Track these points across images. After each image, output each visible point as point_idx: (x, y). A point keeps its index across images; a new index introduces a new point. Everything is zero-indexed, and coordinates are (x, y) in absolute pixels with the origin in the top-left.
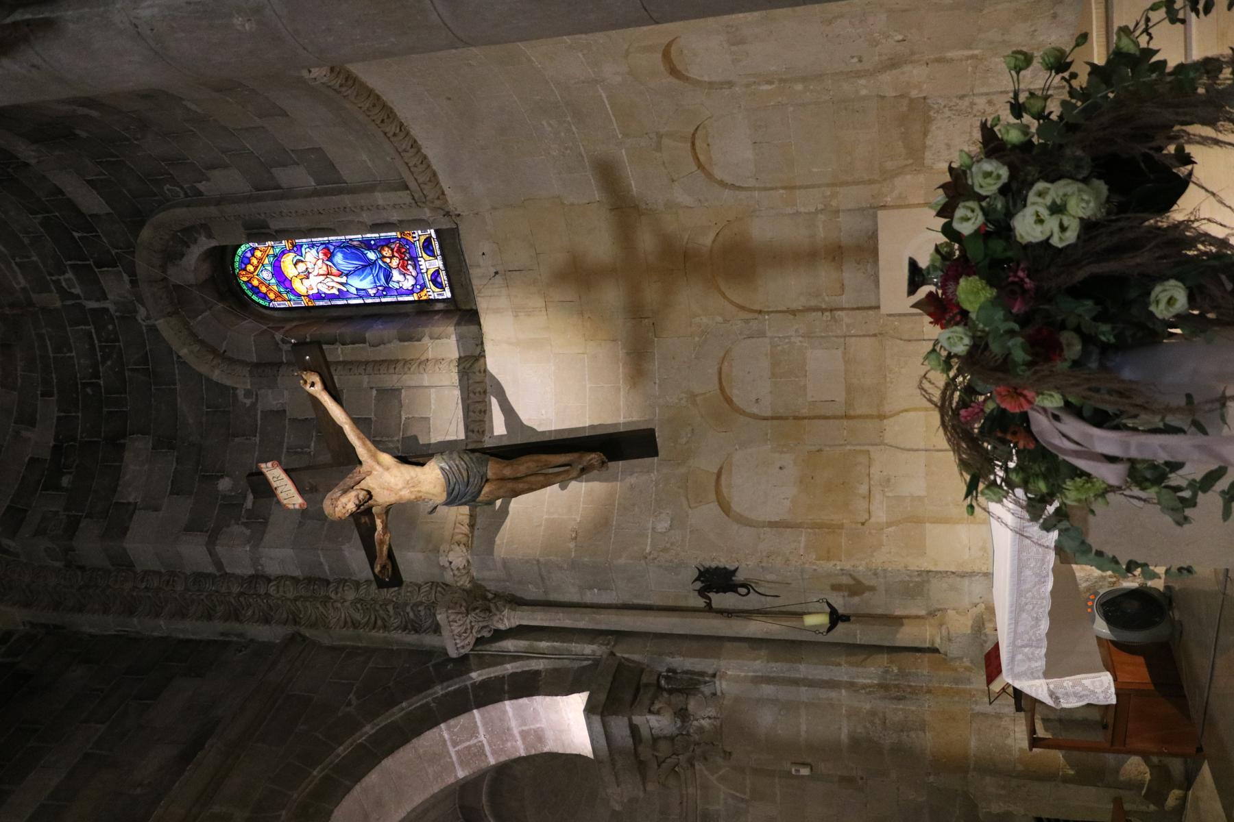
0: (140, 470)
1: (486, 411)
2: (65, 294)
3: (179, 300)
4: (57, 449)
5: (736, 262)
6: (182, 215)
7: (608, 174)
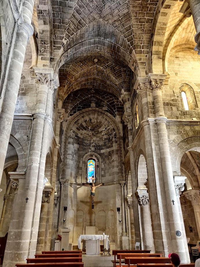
0: (76, 146)
1: (79, 185)
2: (93, 143)
3: (92, 155)
5: (90, 213)
6: (100, 160)
7: (100, 202)
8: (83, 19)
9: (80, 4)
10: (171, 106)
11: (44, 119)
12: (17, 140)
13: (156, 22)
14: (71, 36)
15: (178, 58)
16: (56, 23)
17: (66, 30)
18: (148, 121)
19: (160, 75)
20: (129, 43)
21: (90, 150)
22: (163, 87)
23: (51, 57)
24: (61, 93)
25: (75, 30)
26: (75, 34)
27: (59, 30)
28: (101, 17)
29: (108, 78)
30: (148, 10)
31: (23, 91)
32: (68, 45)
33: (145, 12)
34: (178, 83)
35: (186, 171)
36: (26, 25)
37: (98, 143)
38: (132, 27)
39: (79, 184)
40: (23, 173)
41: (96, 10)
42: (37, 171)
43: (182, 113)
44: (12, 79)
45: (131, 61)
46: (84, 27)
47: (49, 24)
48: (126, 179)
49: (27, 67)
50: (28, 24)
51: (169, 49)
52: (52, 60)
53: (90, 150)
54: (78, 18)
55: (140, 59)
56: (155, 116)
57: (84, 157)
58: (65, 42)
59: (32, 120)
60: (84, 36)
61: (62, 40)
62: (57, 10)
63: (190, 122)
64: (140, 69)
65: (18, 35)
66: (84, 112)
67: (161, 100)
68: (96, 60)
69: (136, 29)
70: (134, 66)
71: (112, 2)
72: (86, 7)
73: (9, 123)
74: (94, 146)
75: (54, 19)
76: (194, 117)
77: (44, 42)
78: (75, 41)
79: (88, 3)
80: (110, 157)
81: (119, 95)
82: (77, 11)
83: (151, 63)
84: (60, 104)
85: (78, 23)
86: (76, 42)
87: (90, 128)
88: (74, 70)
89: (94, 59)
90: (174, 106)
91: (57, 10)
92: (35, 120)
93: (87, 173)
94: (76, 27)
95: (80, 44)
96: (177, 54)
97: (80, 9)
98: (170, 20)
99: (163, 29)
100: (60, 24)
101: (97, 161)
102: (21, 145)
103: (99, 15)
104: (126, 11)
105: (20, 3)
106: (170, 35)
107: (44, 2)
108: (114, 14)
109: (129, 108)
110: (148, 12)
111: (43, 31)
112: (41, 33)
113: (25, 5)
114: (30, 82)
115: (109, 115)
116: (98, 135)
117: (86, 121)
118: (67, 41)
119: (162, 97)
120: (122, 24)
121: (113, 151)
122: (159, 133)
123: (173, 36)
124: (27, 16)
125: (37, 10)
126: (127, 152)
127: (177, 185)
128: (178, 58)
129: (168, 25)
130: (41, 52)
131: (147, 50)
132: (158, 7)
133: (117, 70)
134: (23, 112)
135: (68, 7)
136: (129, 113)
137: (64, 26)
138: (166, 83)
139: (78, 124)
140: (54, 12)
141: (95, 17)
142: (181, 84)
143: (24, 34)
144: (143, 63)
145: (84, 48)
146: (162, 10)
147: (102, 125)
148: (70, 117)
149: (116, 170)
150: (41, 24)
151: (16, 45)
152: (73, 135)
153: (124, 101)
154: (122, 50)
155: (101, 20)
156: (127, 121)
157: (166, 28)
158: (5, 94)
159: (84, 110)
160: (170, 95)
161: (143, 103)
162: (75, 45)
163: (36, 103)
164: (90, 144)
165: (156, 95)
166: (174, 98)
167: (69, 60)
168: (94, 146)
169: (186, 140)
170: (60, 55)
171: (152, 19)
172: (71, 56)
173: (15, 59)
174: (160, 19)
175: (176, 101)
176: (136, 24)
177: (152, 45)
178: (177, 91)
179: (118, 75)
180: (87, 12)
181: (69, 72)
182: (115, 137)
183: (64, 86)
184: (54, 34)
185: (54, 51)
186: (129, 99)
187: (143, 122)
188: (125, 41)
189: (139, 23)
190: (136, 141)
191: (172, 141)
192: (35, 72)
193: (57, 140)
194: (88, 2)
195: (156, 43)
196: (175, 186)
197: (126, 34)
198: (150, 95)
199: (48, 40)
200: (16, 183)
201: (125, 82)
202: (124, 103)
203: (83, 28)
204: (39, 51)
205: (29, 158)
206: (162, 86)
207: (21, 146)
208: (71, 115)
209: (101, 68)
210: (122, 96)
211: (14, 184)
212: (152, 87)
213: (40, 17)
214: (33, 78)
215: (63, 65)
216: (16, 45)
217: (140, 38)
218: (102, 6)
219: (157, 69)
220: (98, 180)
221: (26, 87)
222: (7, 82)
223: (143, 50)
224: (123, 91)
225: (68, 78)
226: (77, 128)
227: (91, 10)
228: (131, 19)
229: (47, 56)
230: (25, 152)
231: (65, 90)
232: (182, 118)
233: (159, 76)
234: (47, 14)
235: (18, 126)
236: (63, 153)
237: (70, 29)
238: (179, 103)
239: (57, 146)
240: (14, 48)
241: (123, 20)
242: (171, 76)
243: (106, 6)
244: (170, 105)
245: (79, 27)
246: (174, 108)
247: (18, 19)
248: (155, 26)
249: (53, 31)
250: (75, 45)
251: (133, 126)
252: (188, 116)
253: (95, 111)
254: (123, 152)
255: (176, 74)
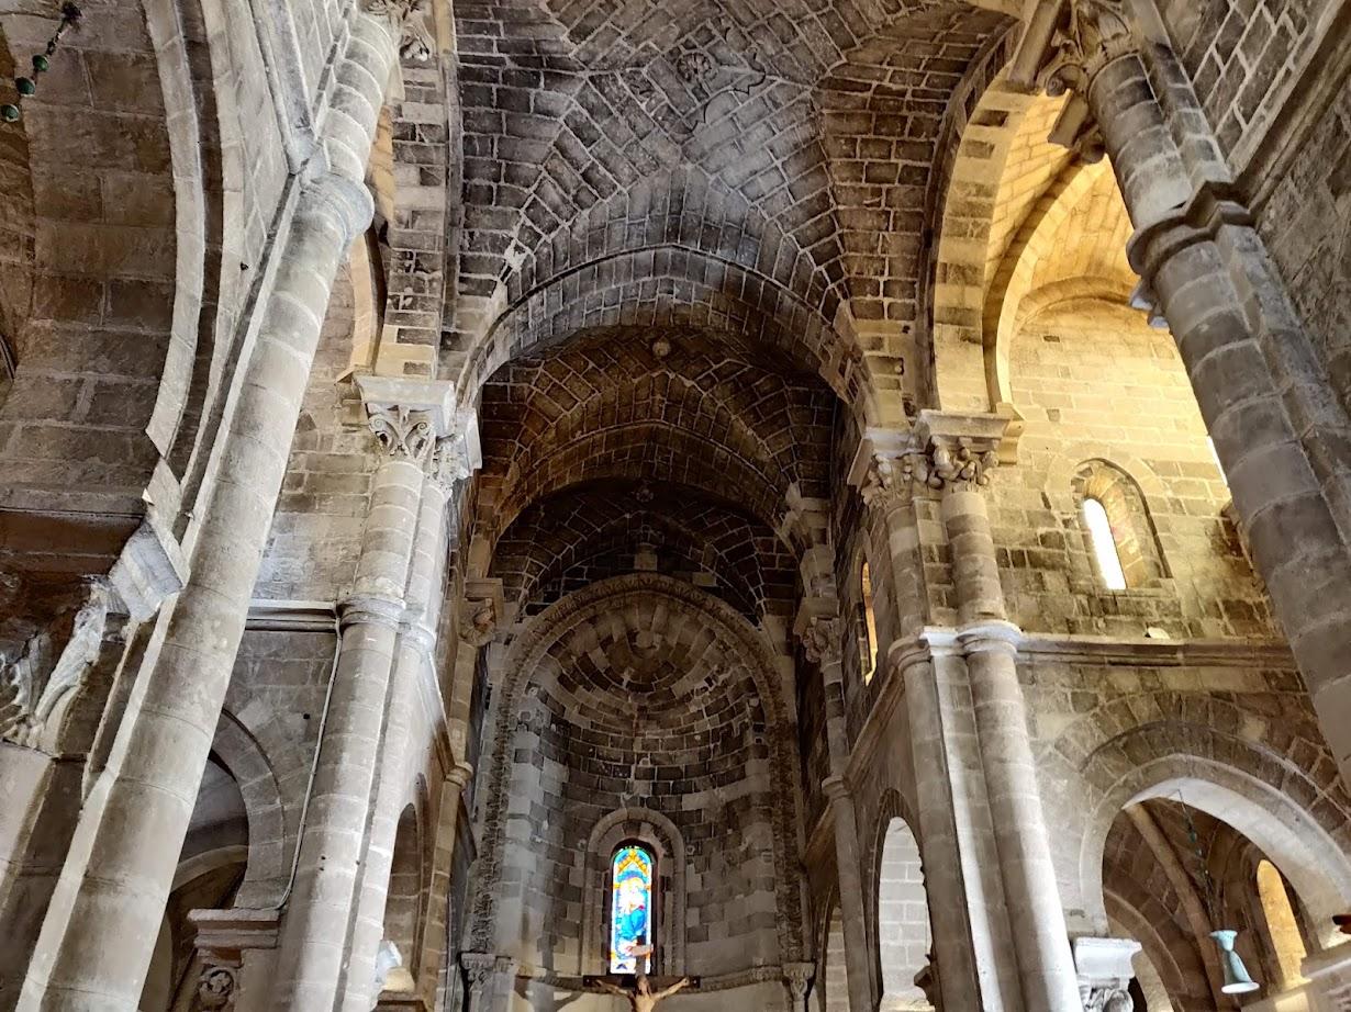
0: (554, 771)
1: (566, 988)
2: (640, 756)
3: (633, 824)
4: (566, 724)
6: (681, 850)
8: (605, 163)
9: (592, 99)
10: (1038, 570)
11: (397, 626)
12: (251, 736)
13: (946, 180)
14: (544, 237)
15: (1057, 339)
16: (476, 181)
17: (522, 211)
18: (923, 644)
19: (973, 419)
20: (822, 268)
21: (628, 797)
22: (993, 476)
23: (446, 329)
24: (486, 503)
25: (565, 210)
26: (566, 225)
27: (492, 207)
28: (686, 155)
29: (721, 429)
30: (907, 131)
31: (300, 491)
32: (528, 274)
33: (893, 139)
34: (1064, 457)
35: (1136, 913)
36: (341, 188)
37: (670, 758)
38: (831, 201)
39: (564, 984)
40: (269, 915)
41: (667, 125)
42: (345, 906)
43: (1093, 604)
44: (255, 427)
45: (830, 350)
46: (610, 199)
47: (444, 184)
48: (814, 950)
49: (326, 374)
50: (351, 183)
51: (1011, 299)
52: (449, 341)
53: (628, 797)
54: (580, 157)
55: (877, 344)
56: (959, 621)
57: (595, 833)
58: (514, 260)
59: (334, 631)
60: (609, 237)
61: (502, 252)
62: (487, 123)
63: (1139, 649)
64: (879, 391)
65: (299, 227)
66: (598, 598)
67: (982, 539)
68: (662, 348)
69: (851, 211)
70: (846, 374)
71: (740, 94)
72: (622, 112)
73: (225, 642)
74: (646, 775)
75: (466, 163)
76: (1155, 625)
77: (417, 263)
78: (566, 259)
79: (630, 98)
80: (730, 831)
81: (777, 515)
82: (578, 131)
83: (927, 361)
84: (481, 554)
85: (580, 178)
86: (568, 263)
87: (626, 678)
88: (556, 392)
89: (653, 341)
90: (1053, 567)
91: (487, 123)
92: (349, 632)
93: (606, 919)
94: (570, 198)
95: (587, 269)
96: (1050, 322)
97: (593, 123)
98: (1006, 175)
99: (978, 211)
100: (497, 180)
101: (660, 856)
102: (268, 762)
103: (679, 147)
104: (803, 133)
105: (320, 96)
106: (1012, 236)
107: (428, 93)
108: (747, 145)
109: (827, 576)
110: (906, 137)
111: (415, 213)
112: (405, 220)
113: (342, 102)
114: (336, 444)
115: (726, 610)
116: (672, 715)
117: (605, 643)
118: (524, 256)
119: (991, 520)
120: (785, 185)
121: (746, 799)
122: (981, 704)
123: (1026, 242)
124: (349, 150)
125: (395, 123)
126: (819, 803)
127: (1094, 985)
128: (1057, 339)
129: (1002, 194)
130: (401, 305)
131: (908, 301)
132: (951, 121)
133: (765, 394)
134: (292, 590)
135: (537, 111)
136: (829, 601)
137: (514, 193)
138: (1006, 457)
139: (569, 654)
140: (472, 133)
141: (662, 154)
142: (1079, 460)
143: (329, 224)
144: (889, 361)
145: (604, 290)
146: (970, 132)
147: (690, 664)
148: (529, 620)
149: (763, 901)
150: (408, 184)
151: (284, 275)
152: (539, 713)
153: (801, 545)
154: (788, 301)
155: (689, 167)
156: (819, 641)
157: (991, 206)
158: (216, 497)
159: (597, 587)
160: (1028, 512)
161: (895, 553)
162: (563, 276)
163: (360, 548)
164: (629, 760)
165: (958, 514)
166: (1050, 530)
167: (533, 344)
168: (646, 775)
169: (1125, 739)
170: (490, 319)
171: (927, 169)
172: (541, 325)
173: (275, 335)
174: (963, 168)
175: (1061, 545)
176: (853, 188)
177: (932, 281)
178: (1062, 495)
179: (767, 420)
180: (624, 131)
181: (532, 403)
182: (758, 729)
183: (505, 469)
184: (466, 226)
185: (461, 304)
186: (824, 532)
187: (901, 649)
188: (800, 261)
189: (863, 184)
190: (863, 744)
191: (1050, 748)
192: (365, 397)
193: (458, 738)
194: (629, 92)
195: (951, 275)
196: (1082, 993)
197: (808, 228)
198: (928, 516)
199: (436, 252)
200: (228, 974)
201: (800, 451)
202: (800, 553)
203: (605, 201)
204: (389, 301)
205: (309, 831)
206: (988, 472)
207: (271, 768)
208: (533, 611)
209: (688, 383)
210: (790, 517)
211: (214, 981)
212: (936, 475)
213: (407, 156)
214: (350, 428)
215: (503, 369)
216: (284, 275)
217: (873, 250)
218: (693, 109)
219: (958, 387)
220: (668, 962)
221: (318, 469)
222: (230, 443)
223: (886, 301)
224: (793, 493)
225: (526, 430)
226: (562, 679)
227: (642, 125)
228: (828, 164)
229: (426, 323)
230: (290, 800)
231: (507, 489)
232: (1095, 629)
233: (969, 421)
234: (439, 142)
235: (263, 661)
236: (484, 810)
237: (543, 204)
238: (1076, 552)
239: (455, 771)
240: (278, 287)
241: (790, 172)
242: (1028, 422)
243: (713, 112)
244: (1034, 565)
245: (584, 196)
246: (1052, 580)
247: (305, 163)
248: (942, 199)
249: (463, 212)
250: (563, 276)
251: (849, 667)
252: (1122, 618)
253: (656, 590)
254: (799, 806)
255: (1053, 414)
